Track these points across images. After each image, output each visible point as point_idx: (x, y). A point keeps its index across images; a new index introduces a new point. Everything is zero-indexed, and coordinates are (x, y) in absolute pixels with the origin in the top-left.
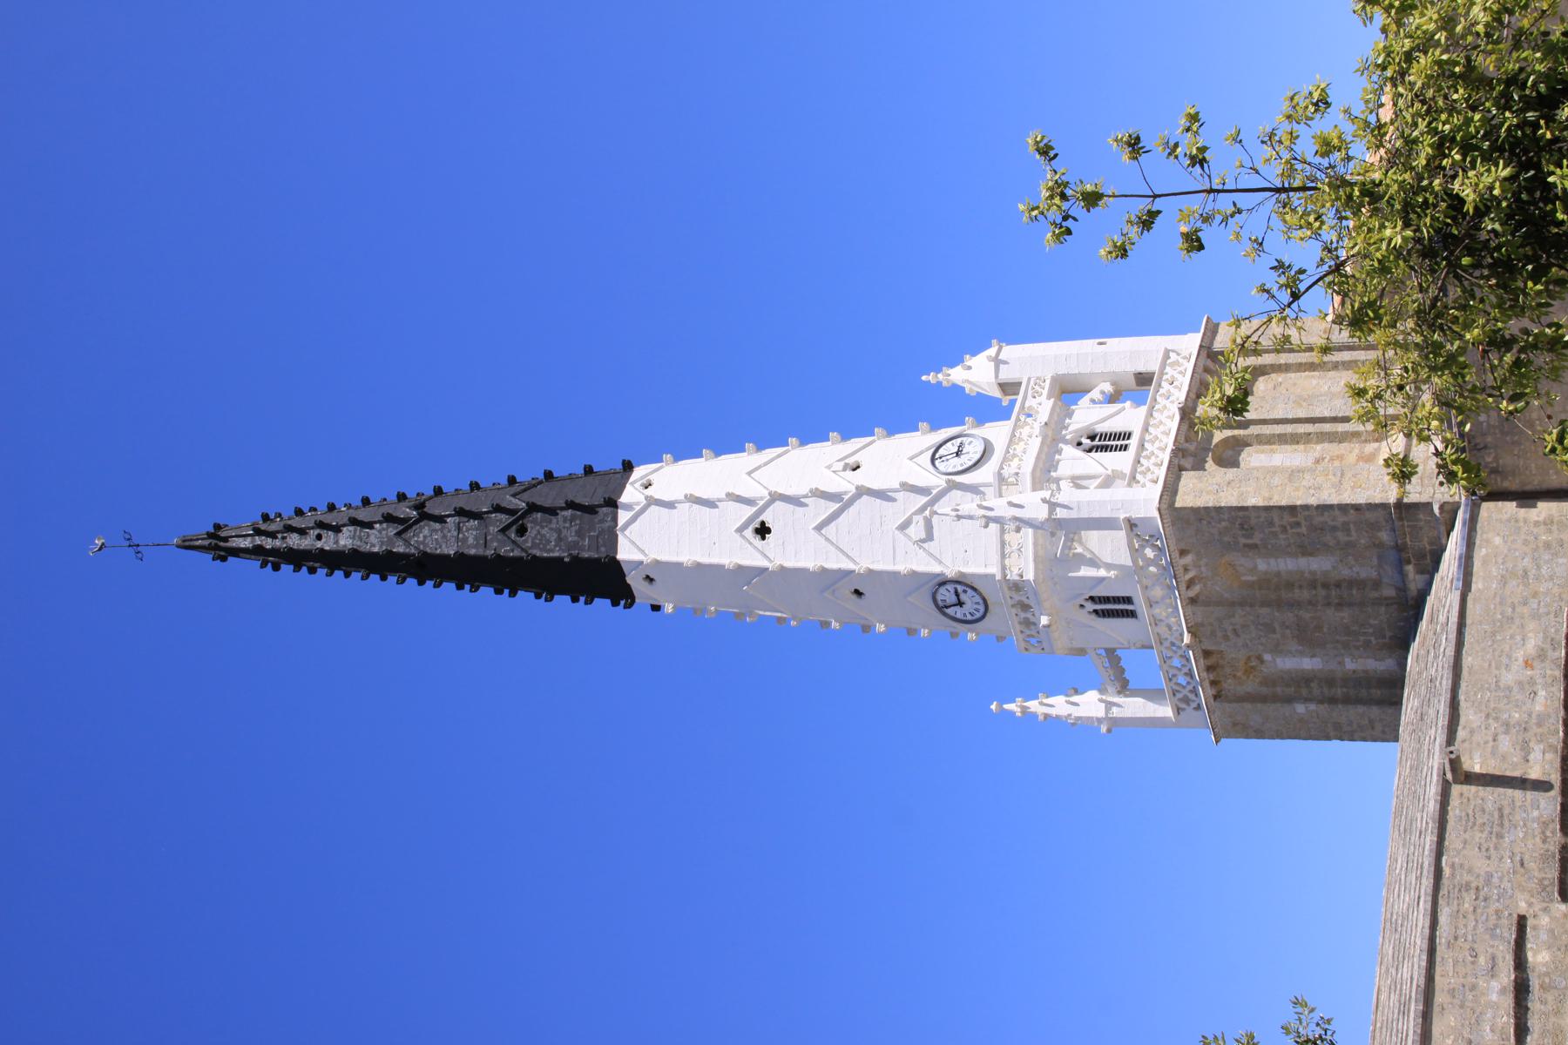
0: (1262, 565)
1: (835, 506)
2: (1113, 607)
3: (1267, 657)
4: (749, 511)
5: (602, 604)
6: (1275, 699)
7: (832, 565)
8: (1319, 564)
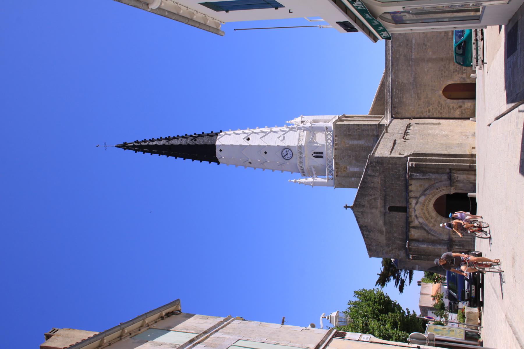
0: (351, 142)
1: (265, 134)
2: (319, 155)
3: (348, 167)
4: (246, 135)
5: (205, 163)
6: (348, 177)
7: (262, 145)
8: (361, 142)
